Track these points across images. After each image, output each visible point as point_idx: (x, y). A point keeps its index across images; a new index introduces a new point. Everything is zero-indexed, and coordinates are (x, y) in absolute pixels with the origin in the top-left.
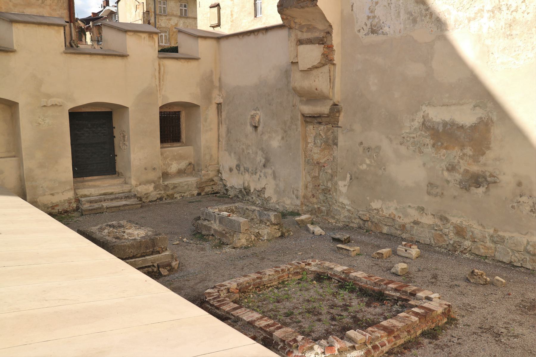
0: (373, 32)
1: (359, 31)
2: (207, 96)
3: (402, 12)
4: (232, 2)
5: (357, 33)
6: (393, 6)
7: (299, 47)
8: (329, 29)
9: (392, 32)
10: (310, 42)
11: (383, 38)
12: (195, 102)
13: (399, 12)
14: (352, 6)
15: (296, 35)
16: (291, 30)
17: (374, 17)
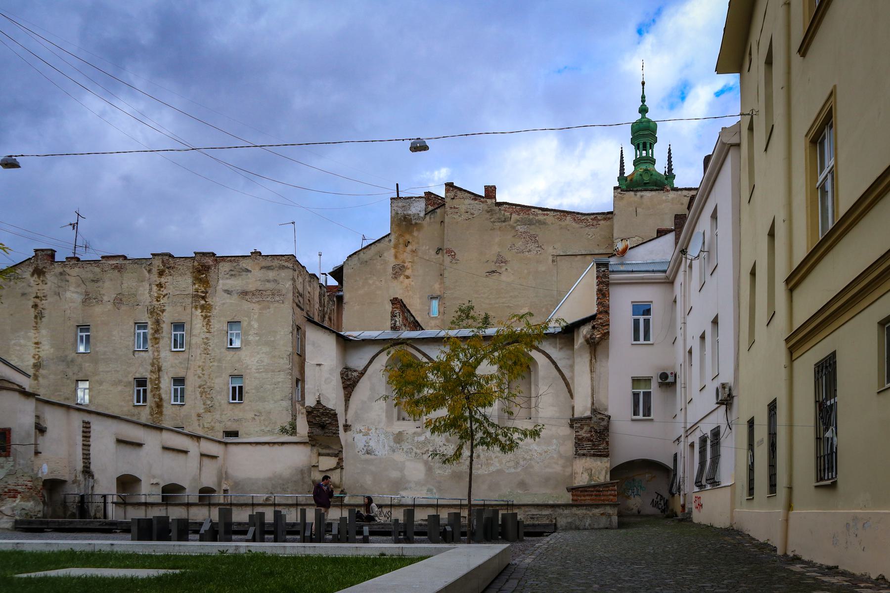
0: (368, 453)
1: (359, 452)
2: (220, 485)
3: (386, 445)
4: (36, 382)
5: (357, 453)
6: (380, 442)
7: (319, 457)
8: (341, 449)
9: (380, 455)
10: (328, 455)
11: (376, 457)
12: (214, 488)
13: (385, 446)
14: (354, 438)
15: (318, 450)
16: (313, 447)
17: (369, 446)
